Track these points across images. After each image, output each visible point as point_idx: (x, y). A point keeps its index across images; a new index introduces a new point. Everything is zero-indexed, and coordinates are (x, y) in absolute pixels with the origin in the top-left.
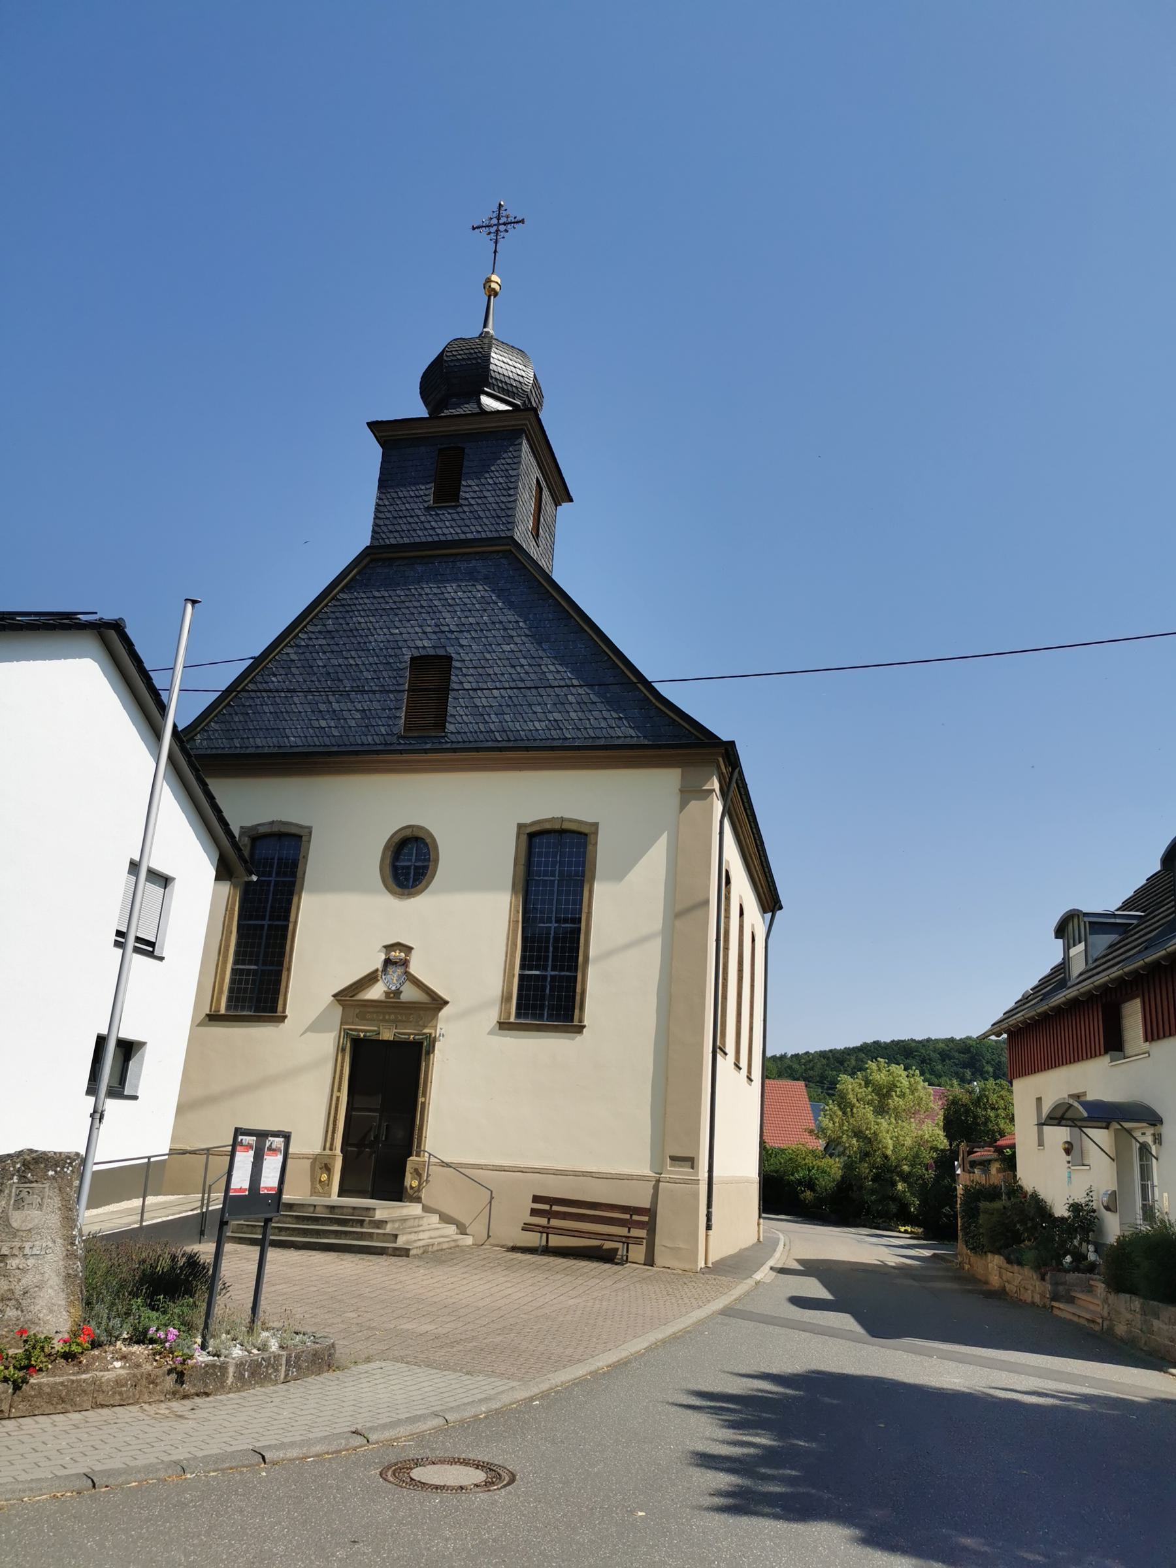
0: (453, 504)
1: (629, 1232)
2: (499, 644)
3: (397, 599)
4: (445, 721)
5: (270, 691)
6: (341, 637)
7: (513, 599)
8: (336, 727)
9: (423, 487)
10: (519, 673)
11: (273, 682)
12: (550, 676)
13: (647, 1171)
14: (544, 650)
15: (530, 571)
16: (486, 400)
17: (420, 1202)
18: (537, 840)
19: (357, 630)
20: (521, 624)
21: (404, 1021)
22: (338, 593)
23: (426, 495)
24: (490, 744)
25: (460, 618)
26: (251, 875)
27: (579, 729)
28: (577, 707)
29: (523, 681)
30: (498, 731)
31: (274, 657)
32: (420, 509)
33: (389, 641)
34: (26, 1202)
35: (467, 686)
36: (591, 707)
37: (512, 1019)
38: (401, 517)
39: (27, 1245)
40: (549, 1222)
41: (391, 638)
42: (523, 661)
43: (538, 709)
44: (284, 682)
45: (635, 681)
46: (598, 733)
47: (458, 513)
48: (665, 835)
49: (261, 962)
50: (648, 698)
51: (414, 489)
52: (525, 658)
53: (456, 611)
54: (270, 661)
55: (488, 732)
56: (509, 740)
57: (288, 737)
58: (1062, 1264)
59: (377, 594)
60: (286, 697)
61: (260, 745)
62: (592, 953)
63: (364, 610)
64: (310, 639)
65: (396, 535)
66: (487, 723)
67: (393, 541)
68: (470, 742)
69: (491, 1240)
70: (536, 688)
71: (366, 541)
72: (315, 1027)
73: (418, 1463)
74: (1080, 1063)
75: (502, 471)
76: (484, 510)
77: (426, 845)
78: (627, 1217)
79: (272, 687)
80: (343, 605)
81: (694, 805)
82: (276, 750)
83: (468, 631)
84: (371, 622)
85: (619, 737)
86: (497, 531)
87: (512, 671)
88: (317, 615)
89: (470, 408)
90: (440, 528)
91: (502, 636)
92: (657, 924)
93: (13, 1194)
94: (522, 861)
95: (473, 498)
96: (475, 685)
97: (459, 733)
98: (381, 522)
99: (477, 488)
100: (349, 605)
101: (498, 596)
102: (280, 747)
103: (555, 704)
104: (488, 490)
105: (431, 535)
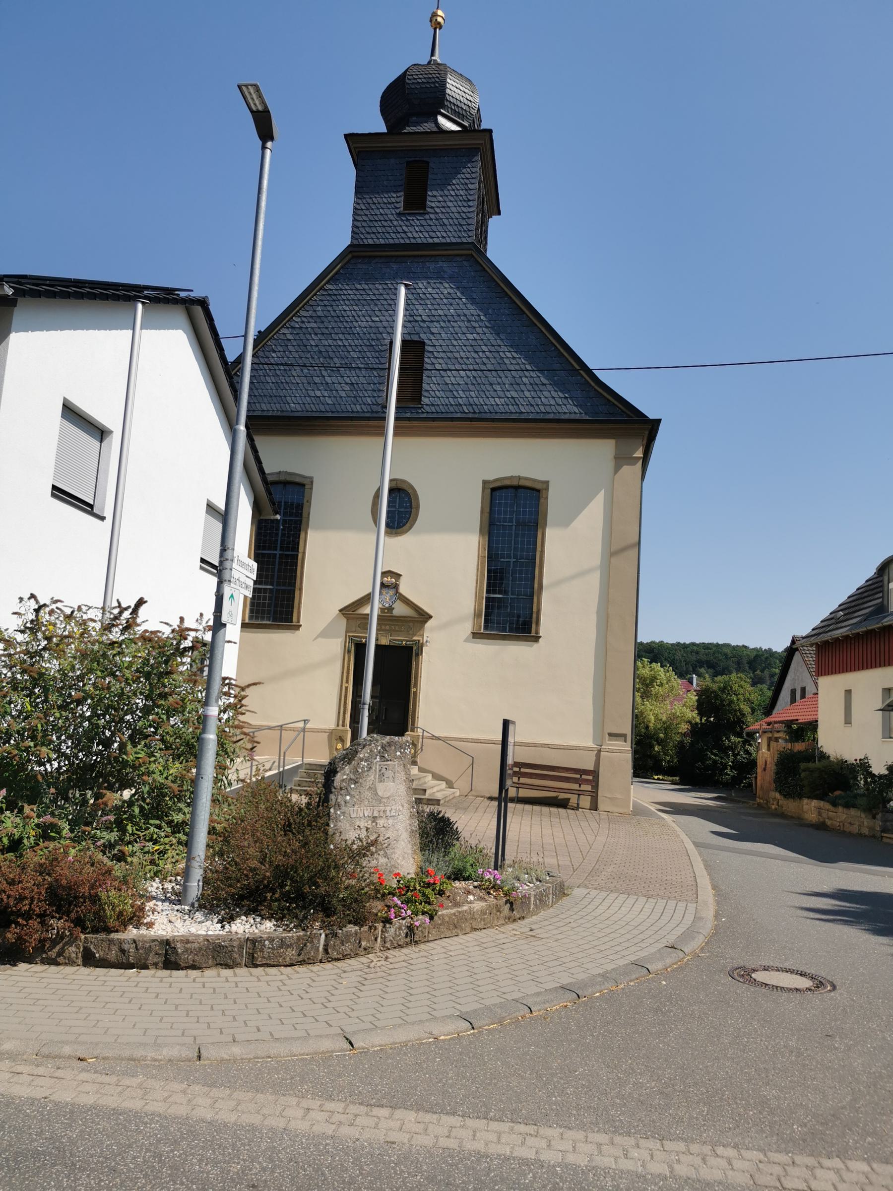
0: (421, 211)
1: (580, 787)
2: (464, 334)
3: (376, 292)
4: (421, 395)
5: (271, 364)
6: (330, 322)
7: (475, 296)
8: (330, 397)
9: (394, 195)
10: (481, 358)
11: (273, 357)
12: (507, 361)
13: (590, 744)
14: (502, 340)
15: (488, 273)
16: (442, 120)
17: (416, 765)
18: (498, 493)
19: (343, 316)
20: (482, 317)
21: (397, 631)
22: (325, 285)
23: (397, 203)
24: (459, 415)
25: (430, 310)
26: (276, 514)
27: (532, 405)
28: (530, 388)
29: (485, 364)
30: (465, 405)
31: (273, 336)
32: (393, 214)
33: (371, 327)
34: (385, 776)
35: (438, 367)
36: (542, 388)
37: (482, 631)
38: (376, 221)
39: (388, 809)
40: (519, 780)
41: (373, 324)
42: (484, 348)
43: (498, 388)
44: (283, 358)
45: (578, 368)
46: (548, 409)
47: (425, 219)
48: (603, 492)
49: (275, 584)
50: (588, 382)
51: (387, 196)
52: (486, 345)
53: (427, 304)
54: (269, 340)
55: (456, 405)
56: (475, 413)
57: (289, 403)
58: (886, 807)
59: (358, 287)
60: (285, 370)
61: (265, 409)
62: (545, 581)
63: (348, 300)
64: (303, 322)
65: (373, 236)
66: (456, 398)
67: (370, 242)
68: (442, 413)
69: (473, 793)
70: (496, 370)
71: (347, 241)
72: (324, 634)
73: (754, 970)
74: (884, 668)
75: (462, 184)
76: (448, 219)
77: (408, 494)
78: (578, 776)
79: (272, 361)
80: (330, 295)
81: (626, 469)
82: (279, 414)
83: (438, 321)
84: (355, 310)
85: (565, 413)
86: (459, 237)
87: (476, 355)
88: (308, 302)
89: (428, 127)
90: (411, 232)
91: (467, 327)
92: (597, 561)
93: (378, 770)
94: (487, 510)
95: (438, 207)
96: (445, 367)
97: (433, 405)
98: (359, 224)
99: (441, 199)
100: (335, 295)
101: (462, 293)
102: (282, 411)
103: (512, 384)
104: (451, 201)
105: (403, 238)
